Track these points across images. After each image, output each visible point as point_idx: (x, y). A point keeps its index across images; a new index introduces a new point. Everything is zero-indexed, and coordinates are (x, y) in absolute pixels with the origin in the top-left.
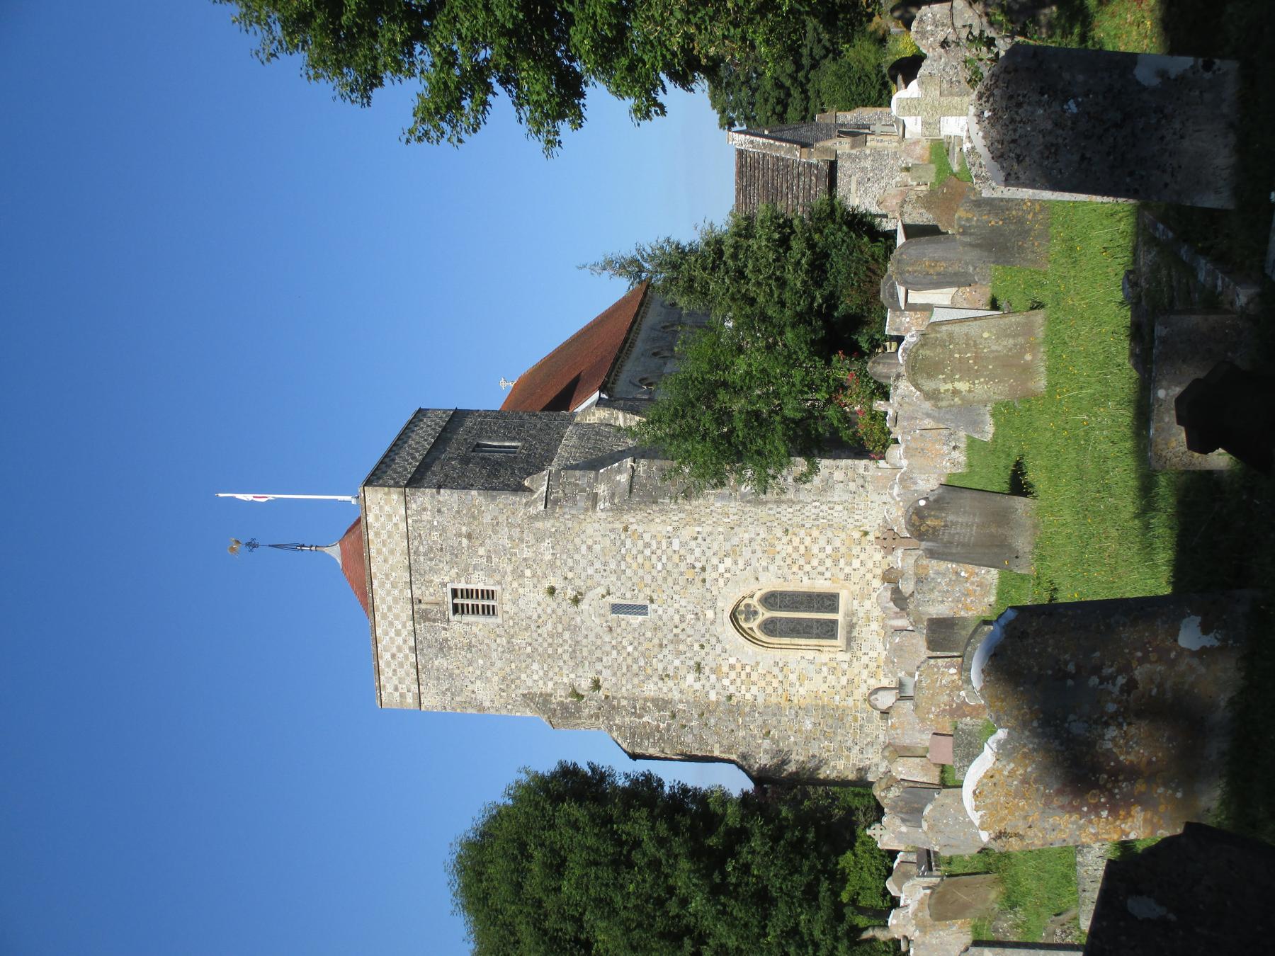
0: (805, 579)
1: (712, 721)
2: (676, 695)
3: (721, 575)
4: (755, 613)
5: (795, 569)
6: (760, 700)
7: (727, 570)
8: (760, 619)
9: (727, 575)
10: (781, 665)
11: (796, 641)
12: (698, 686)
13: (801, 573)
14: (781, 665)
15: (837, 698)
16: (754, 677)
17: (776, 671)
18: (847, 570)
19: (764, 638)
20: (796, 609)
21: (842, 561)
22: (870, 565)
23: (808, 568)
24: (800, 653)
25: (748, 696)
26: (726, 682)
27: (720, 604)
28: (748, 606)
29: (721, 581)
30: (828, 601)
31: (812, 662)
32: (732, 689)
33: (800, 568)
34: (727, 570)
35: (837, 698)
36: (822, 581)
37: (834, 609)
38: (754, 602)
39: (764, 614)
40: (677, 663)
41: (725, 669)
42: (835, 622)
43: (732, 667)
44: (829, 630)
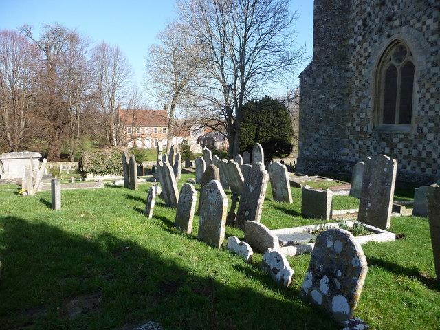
0: (419, 95)
1: (334, 44)
2: (351, 17)
3: (424, 23)
4: (400, 60)
5: (428, 85)
6: (349, 74)
7: (428, 27)
8: (396, 64)
9: (424, 27)
10: (367, 84)
11: (382, 94)
12: (356, 29)
13: (424, 91)
14: (367, 84)
15: (349, 125)
16: (361, 67)
17: (363, 81)
18: (425, 130)
19: (385, 69)
20: (402, 91)
21: (432, 125)
22: (430, 148)
23: (428, 96)
24: (372, 97)
25: (351, 65)
26: (358, 48)
27: (404, 29)
28: (405, 53)
29: (419, 25)
30: (406, 118)
31: (367, 107)
32: (355, 53)
33: (428, 90)
34: (428, 27)
35: (349, 125)
36: (417, 109)
37: (401, 122)
38: (407, 58)
39: (399, 66)
40: (369, 9)
41: (365, 45)
42: (394, 123)
43: (365, 50)
44: (389, 118)
